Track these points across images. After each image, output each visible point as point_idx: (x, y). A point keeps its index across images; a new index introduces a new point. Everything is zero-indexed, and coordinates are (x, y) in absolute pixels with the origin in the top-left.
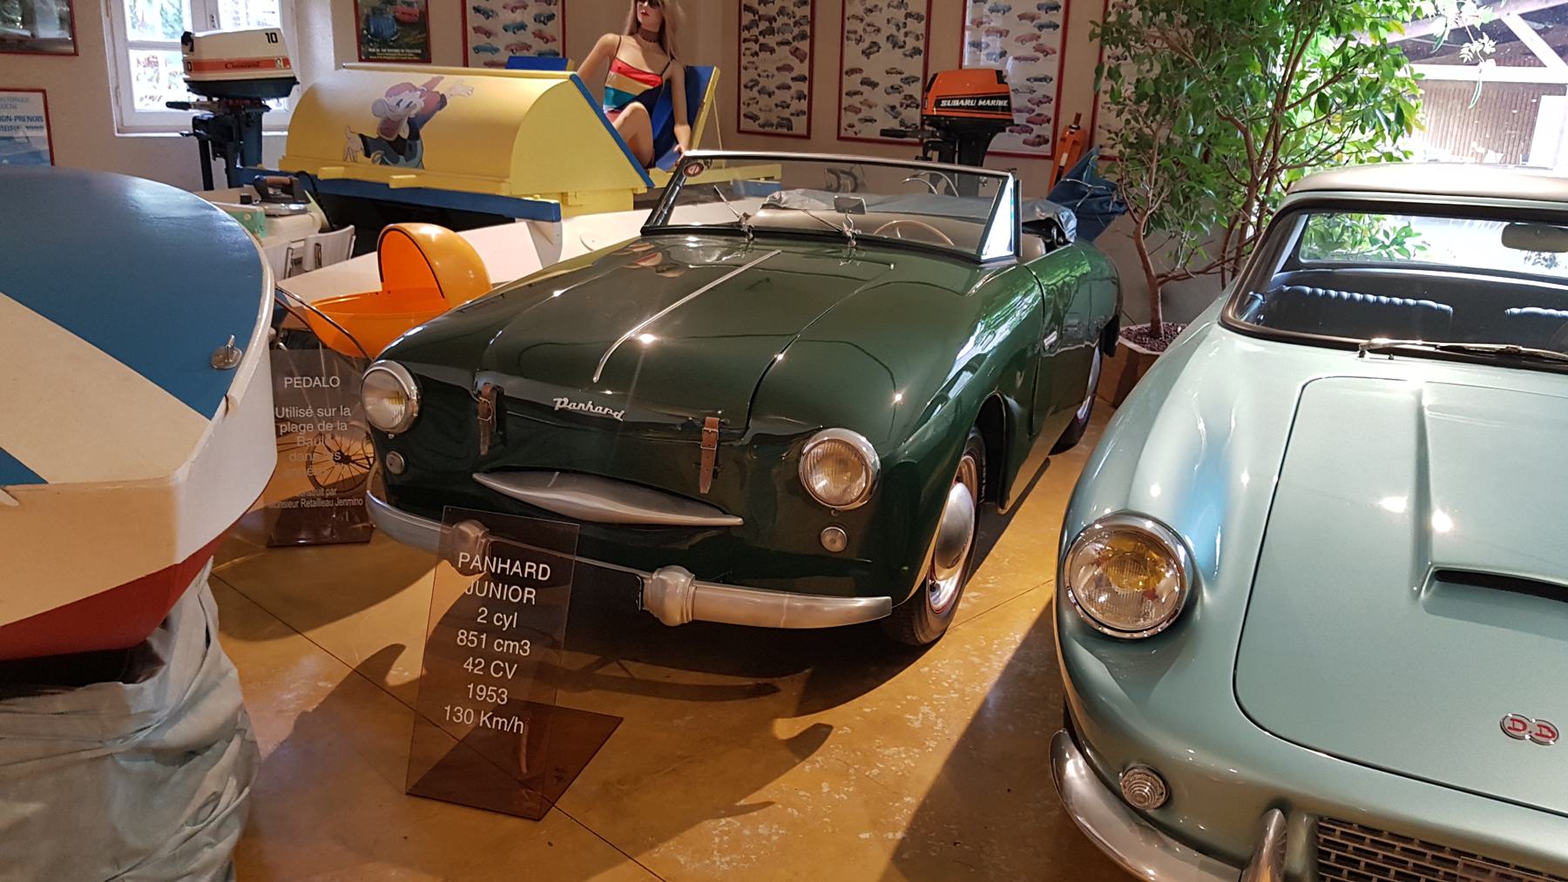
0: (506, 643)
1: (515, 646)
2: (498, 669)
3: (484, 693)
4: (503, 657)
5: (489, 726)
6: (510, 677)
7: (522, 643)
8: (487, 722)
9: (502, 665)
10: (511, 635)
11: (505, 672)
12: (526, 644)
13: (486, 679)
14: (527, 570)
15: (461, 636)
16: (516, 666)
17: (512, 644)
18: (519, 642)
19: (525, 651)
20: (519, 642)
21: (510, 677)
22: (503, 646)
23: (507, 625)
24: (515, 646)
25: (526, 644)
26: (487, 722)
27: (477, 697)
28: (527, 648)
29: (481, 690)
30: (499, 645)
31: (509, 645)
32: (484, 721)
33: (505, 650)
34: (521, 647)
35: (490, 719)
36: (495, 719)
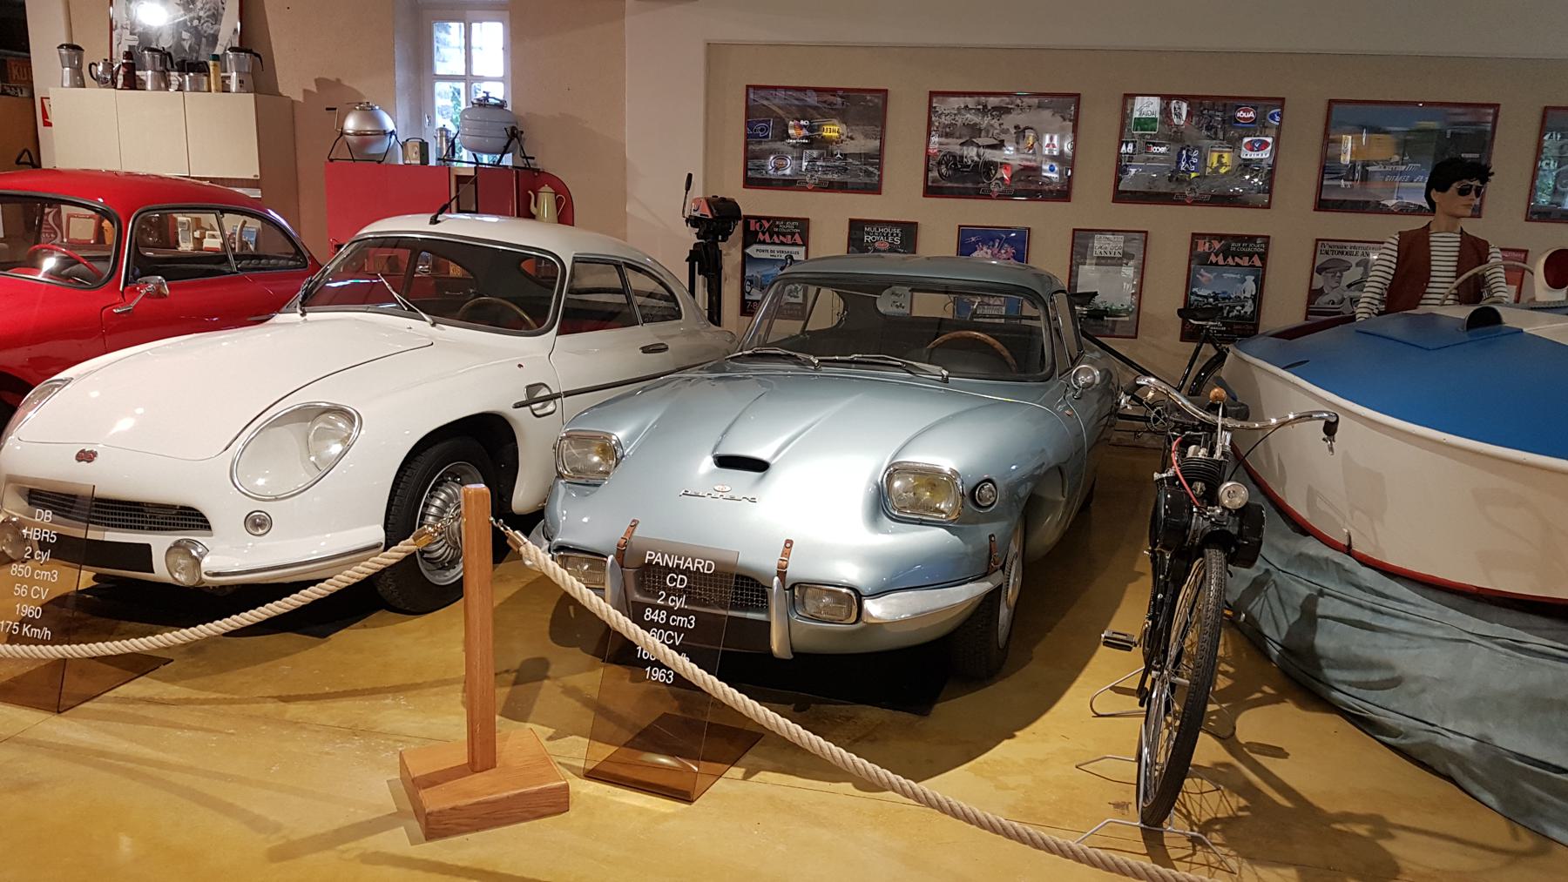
0: (679, 618)
1: (684, 621)
4: (674, 629)
6: (677, 644)
9: (673, 634)
10: (681, 612)
12: (692, 619)
14: (696, 565)
15: (647, 613)
17: (682, 619)
21: (677, 644)
23: (678, 605)
24: (684, 621)
25: (692, 619)
28: (692, 622)
30: (674, 620)
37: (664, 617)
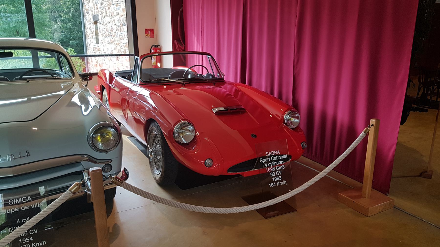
1: (281, 167)
2: (278, 173)
3: (277, 179)
5: (279, 185)
6: (281, 174)
7: (283, 166)
8: (279, 184)
11: (279, 174)
12: (283, 166)
13: (276, 176)
16: (281, 171)
18: (282, 166)
19: (284, 168)
20: (282, 166)
22: (279, 168)
24: (281, 167)
25: (283, 166)
26: (279, 184)
27: (275, 180)
29: (276, 178)
31: (280, 167)
32: (278, 184)
33: (280, 169)
34: (283, 167)
35: (279, 183)
36: (280, 183)
37: (274, 169)
